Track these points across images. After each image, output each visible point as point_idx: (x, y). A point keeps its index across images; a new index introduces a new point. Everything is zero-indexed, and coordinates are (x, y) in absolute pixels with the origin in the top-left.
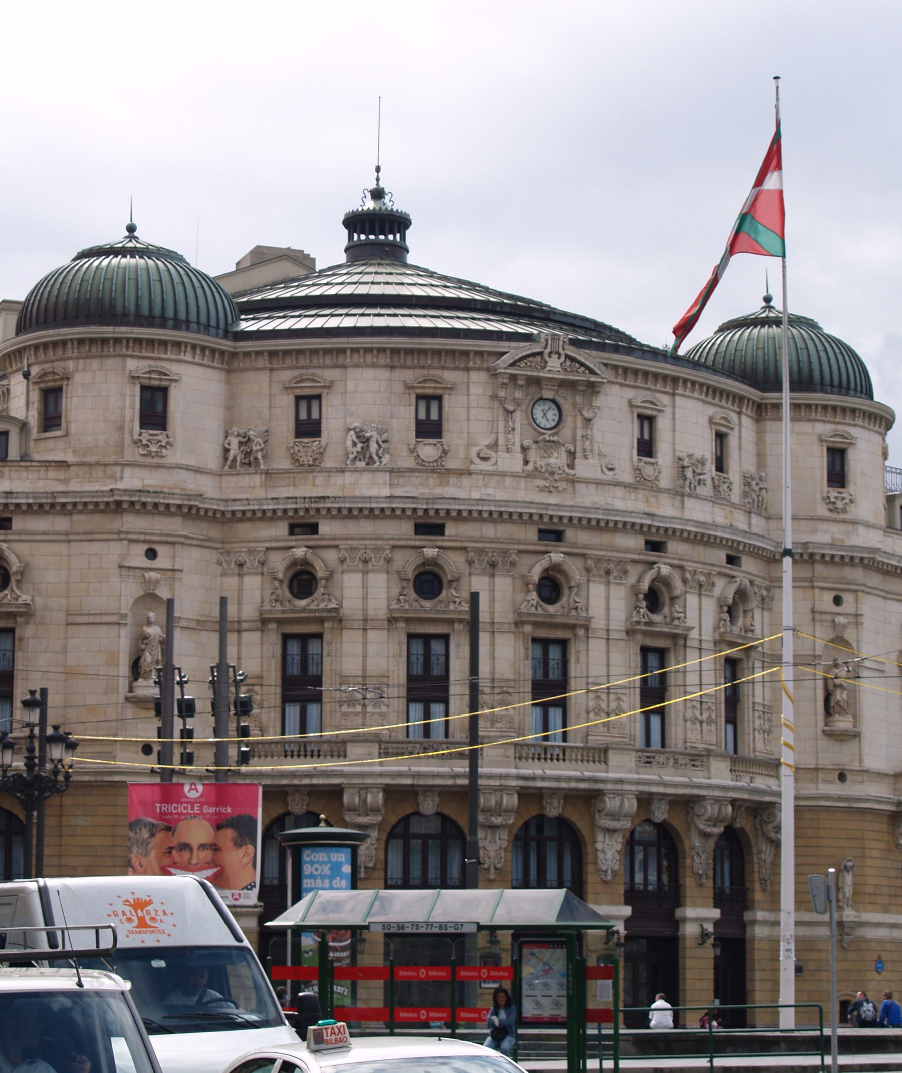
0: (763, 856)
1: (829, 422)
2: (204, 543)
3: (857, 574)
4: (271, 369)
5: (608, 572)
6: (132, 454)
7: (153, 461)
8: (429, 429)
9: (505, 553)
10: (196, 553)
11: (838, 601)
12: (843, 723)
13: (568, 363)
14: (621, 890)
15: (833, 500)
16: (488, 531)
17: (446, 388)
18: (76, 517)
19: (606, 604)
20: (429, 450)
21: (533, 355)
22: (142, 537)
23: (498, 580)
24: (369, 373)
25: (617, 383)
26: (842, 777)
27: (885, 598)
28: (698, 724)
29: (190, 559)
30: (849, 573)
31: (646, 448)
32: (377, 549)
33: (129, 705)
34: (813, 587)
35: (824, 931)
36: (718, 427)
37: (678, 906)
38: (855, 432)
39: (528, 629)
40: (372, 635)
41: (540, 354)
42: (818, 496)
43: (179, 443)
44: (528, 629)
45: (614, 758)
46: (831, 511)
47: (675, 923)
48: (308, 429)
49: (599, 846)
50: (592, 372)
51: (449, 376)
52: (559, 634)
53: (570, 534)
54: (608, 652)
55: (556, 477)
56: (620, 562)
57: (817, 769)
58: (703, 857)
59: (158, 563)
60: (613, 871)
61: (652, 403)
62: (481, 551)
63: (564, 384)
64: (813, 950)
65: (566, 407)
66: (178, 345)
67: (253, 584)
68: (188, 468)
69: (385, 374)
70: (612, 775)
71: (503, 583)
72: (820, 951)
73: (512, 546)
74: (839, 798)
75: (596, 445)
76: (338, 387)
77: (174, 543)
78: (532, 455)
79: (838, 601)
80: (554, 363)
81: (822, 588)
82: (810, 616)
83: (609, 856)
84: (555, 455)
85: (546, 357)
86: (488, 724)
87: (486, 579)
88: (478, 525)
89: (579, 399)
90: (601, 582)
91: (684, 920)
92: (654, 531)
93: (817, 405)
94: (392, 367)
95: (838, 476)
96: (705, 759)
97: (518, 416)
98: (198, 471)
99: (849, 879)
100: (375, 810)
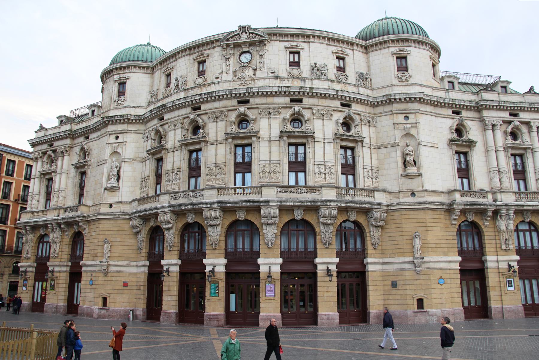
0: (372, 233)
1: (396, 47)
2: (136, 132)
3: (416, 106)
4: (161, 69)
5: (270, 113)
6: (113, 105)
7: (120, 106)
8: (201, 73)
9: (222, 112)
10: (133, 135)
11: (407, 118)
12: (412, 170)
13: (251, 35)
15: (400, 77)
16: (217, 104)
17: (206, 56)
18: (102, 130)
19: (269, 127)
20: (200, 81)
21: (236, 35)
22: (113, 132)
23: (220, 123)
24: (183, 59)
25: (277, 40)
26: (413, 194)
27: (436, 116)
28: (323, 175)
29: (129, 138)
30: (411, 106)
31: (295, 64)
32: (178, 120)
33: (106, 191)
34: (393, 114)
35: (407, 266)
36: (337, 54)
37: (365, 258)
38: (408, 49)
39: (230, 140)
40: (177, 153)
41: (239, 34)
43: (128, 99)
44: (230, 140)
45: (265, 191)
46: (400, 81)
47: (315, 266)
48: (168, 85)
49: (265, 232)
50: (261, 36)
51: (207, 52)
52: (246, 141)
53: (252, 100)
54: (269, 146)
55: (246, 79)
56: (275, 108)
57: (399, 192)
58: (327, 234)
59: (119, 140)
60: (272, 243)
61: (296, 46)
62: (212, 113)
63: (251, 44)
64: (402, 275)
65: (254, 53)
66: (129, 67)
67: (149, 141)
68: (133, 107)
69: (187, 58)
70: (263, 198)
71: (222, 124)
72: (405, 275)
73: (225, 109)
74: (410, 204)
75: (265, 65)
76: (175, 68)
77: (124, 133)
78: (238, 74)
79: (407, 118)
80: (244, 36)
81: (397, 114)
82: (393, 126)
83: (270, 236)
84: (247, 71)
85: (240, 34)
86: (214, 182)
87: (215, 123)
88: (212, 103)
89: (258, 48)
90: (266, 118)
91: (367, 263)
92: (292, 93)
93: (389, 41)
94: (190, 55)
95: (403, 68)
96: (320, 189)
97: (231, 59)
98: (135, 107)
99: (418, 242)
100: (169, 222)
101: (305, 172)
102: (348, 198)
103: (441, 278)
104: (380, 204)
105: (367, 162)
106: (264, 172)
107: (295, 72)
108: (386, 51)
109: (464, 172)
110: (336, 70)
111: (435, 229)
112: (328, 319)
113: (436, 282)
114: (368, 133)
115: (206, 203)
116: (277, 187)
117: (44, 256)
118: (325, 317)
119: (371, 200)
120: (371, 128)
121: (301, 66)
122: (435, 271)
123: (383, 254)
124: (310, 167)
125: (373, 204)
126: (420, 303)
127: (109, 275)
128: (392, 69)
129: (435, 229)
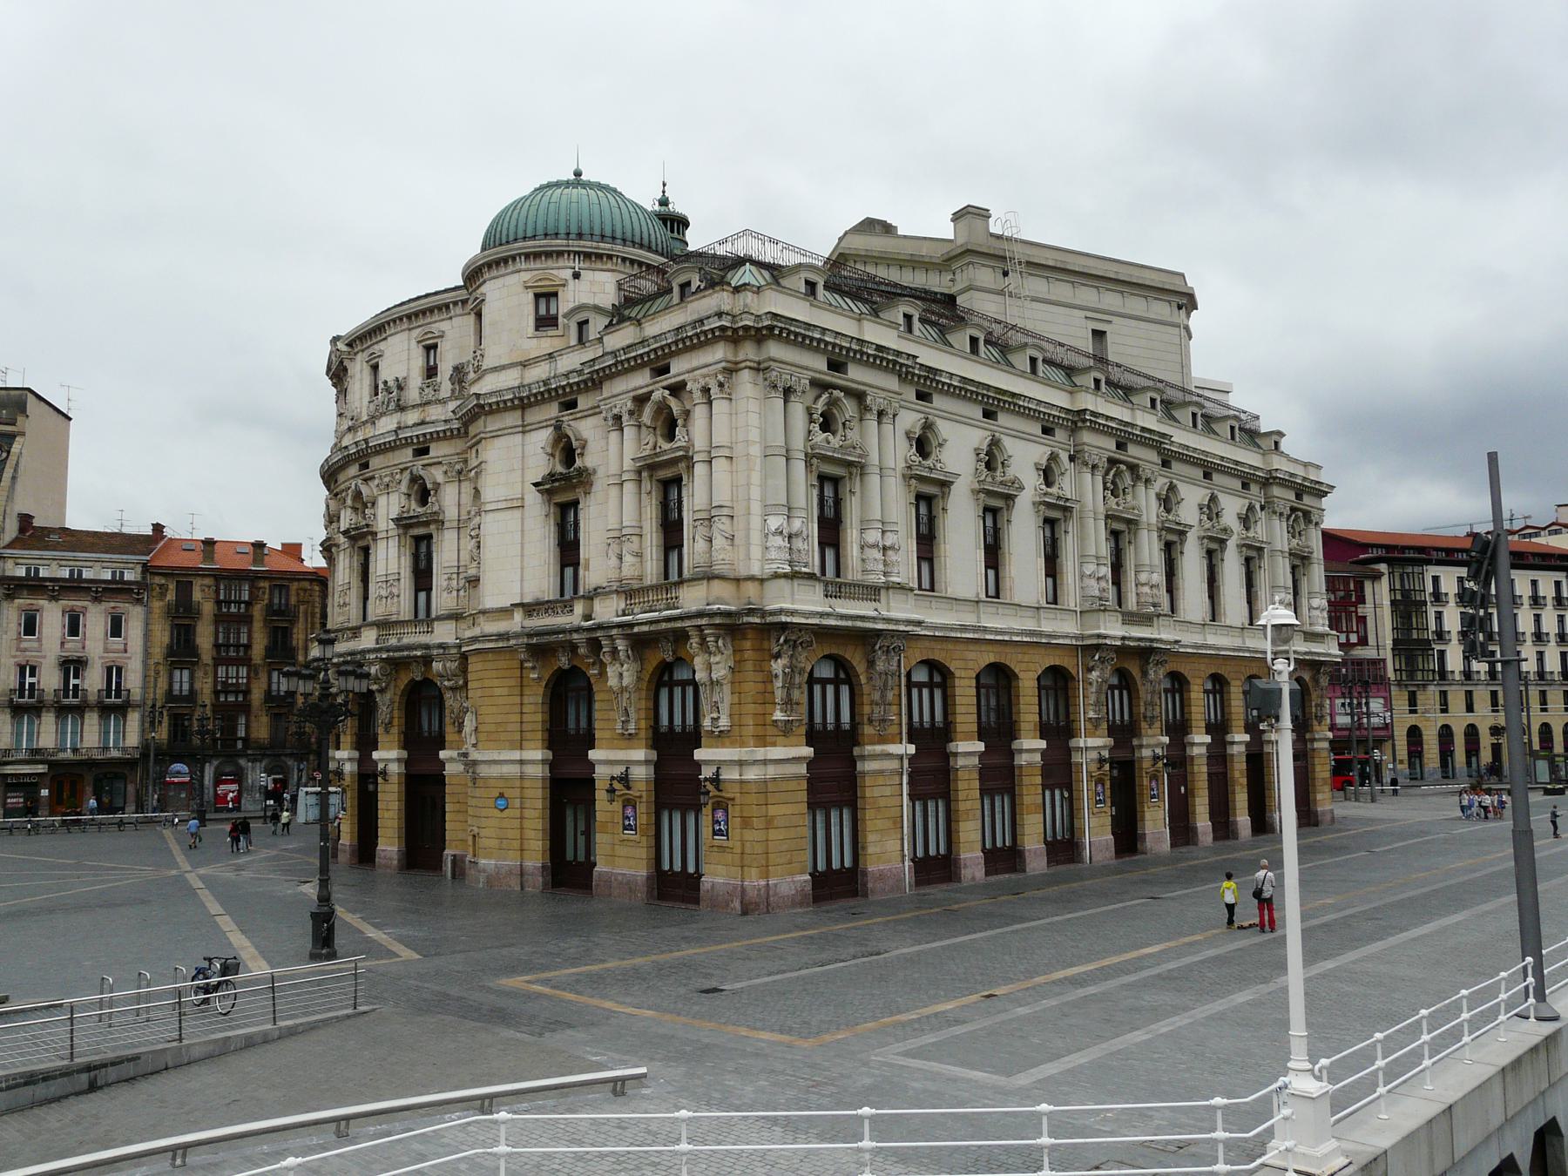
102: (393, 641)
103: (502, 796)
109: (568, 551)
111: (498, 691)
113: (491, 803)
117: (830, 727)
119: (424, 639)
122: (492, 783)
125: (427, 647)
129: (498, 691)
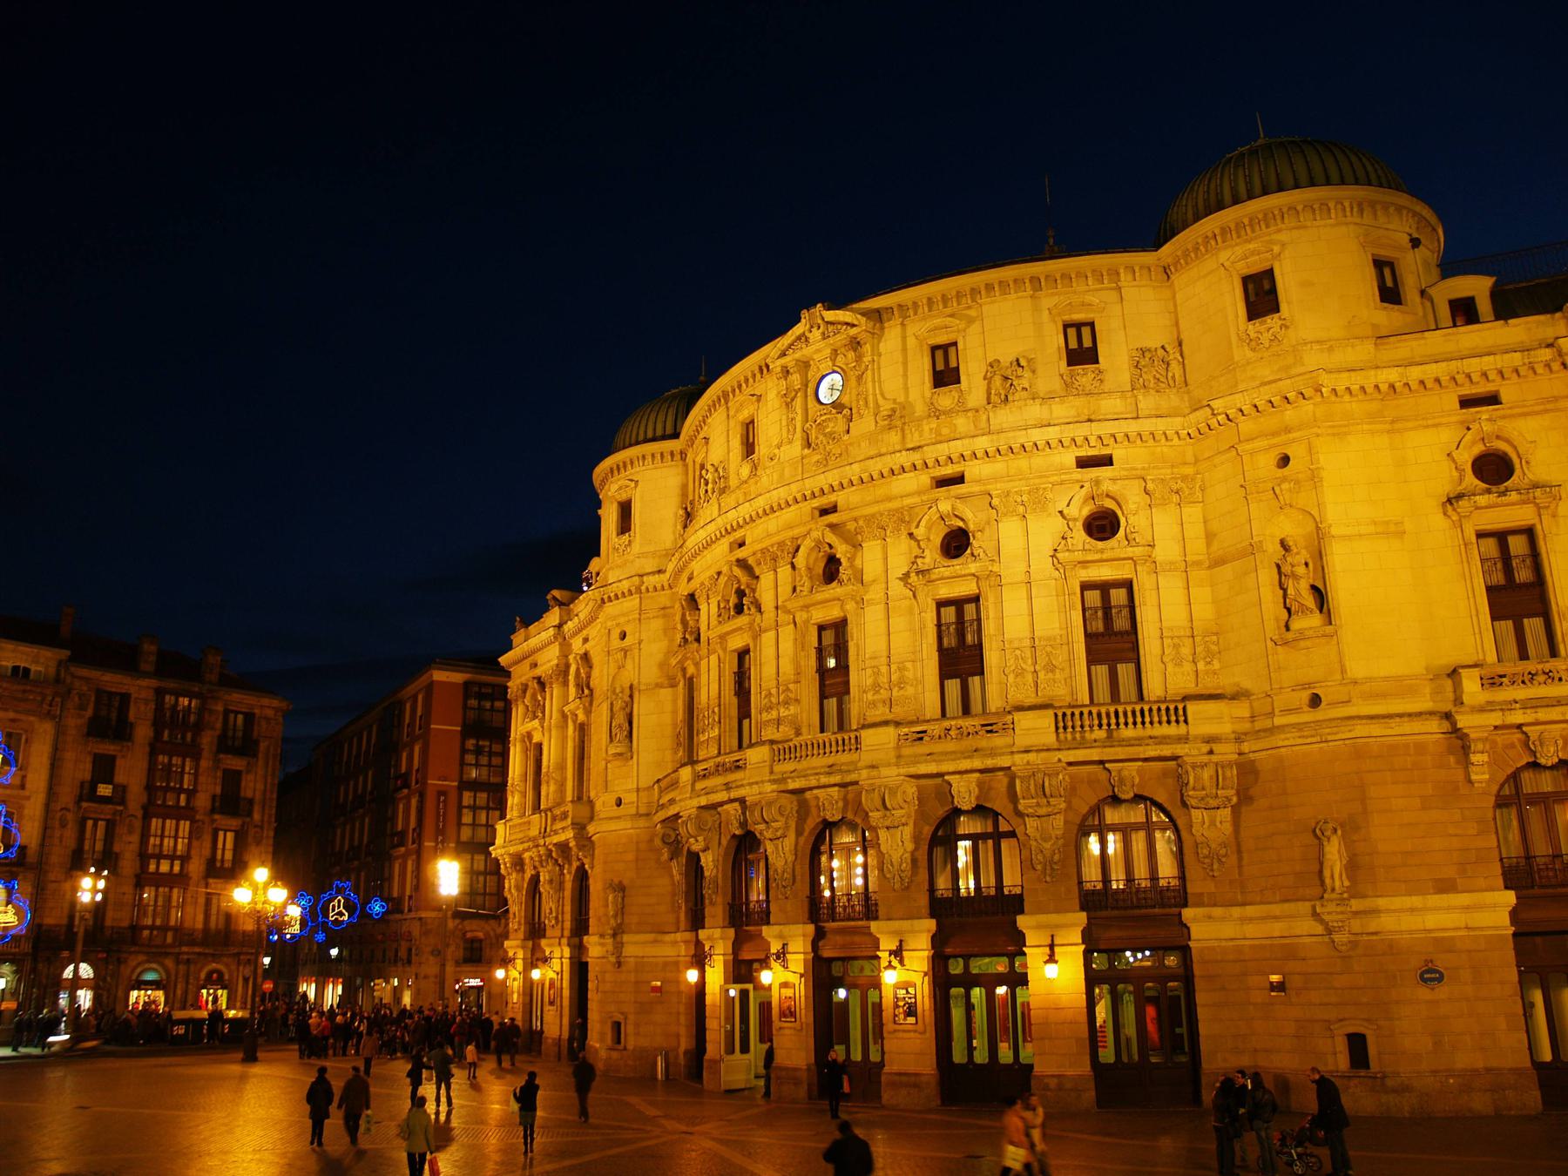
8: (749, 448)
9: (781, 544)
13: (831, 328)
14: (923, 901)
21: (799, 338)
42: (1234, 339)
50: (853, 326)
56: (892, 513)
99: (1334, 852)
101: (982, 673)
104: (1210, 740)
105: (1175, 615)
106: (876, 687)
107: (946, 397)
108: (1210, 263)
110: (1064, 363)
112: (1060, 1087)
114: (1177, 529)
115: (750, 784)
116: (897, 724)
118: (1053, 1083)
120: (1187, 510)
121: (963, 378)
123: (1238, 894)
124: (991, 657)
126: (1357, 1044)
127: (623, 968)
128: (1231, 317)
